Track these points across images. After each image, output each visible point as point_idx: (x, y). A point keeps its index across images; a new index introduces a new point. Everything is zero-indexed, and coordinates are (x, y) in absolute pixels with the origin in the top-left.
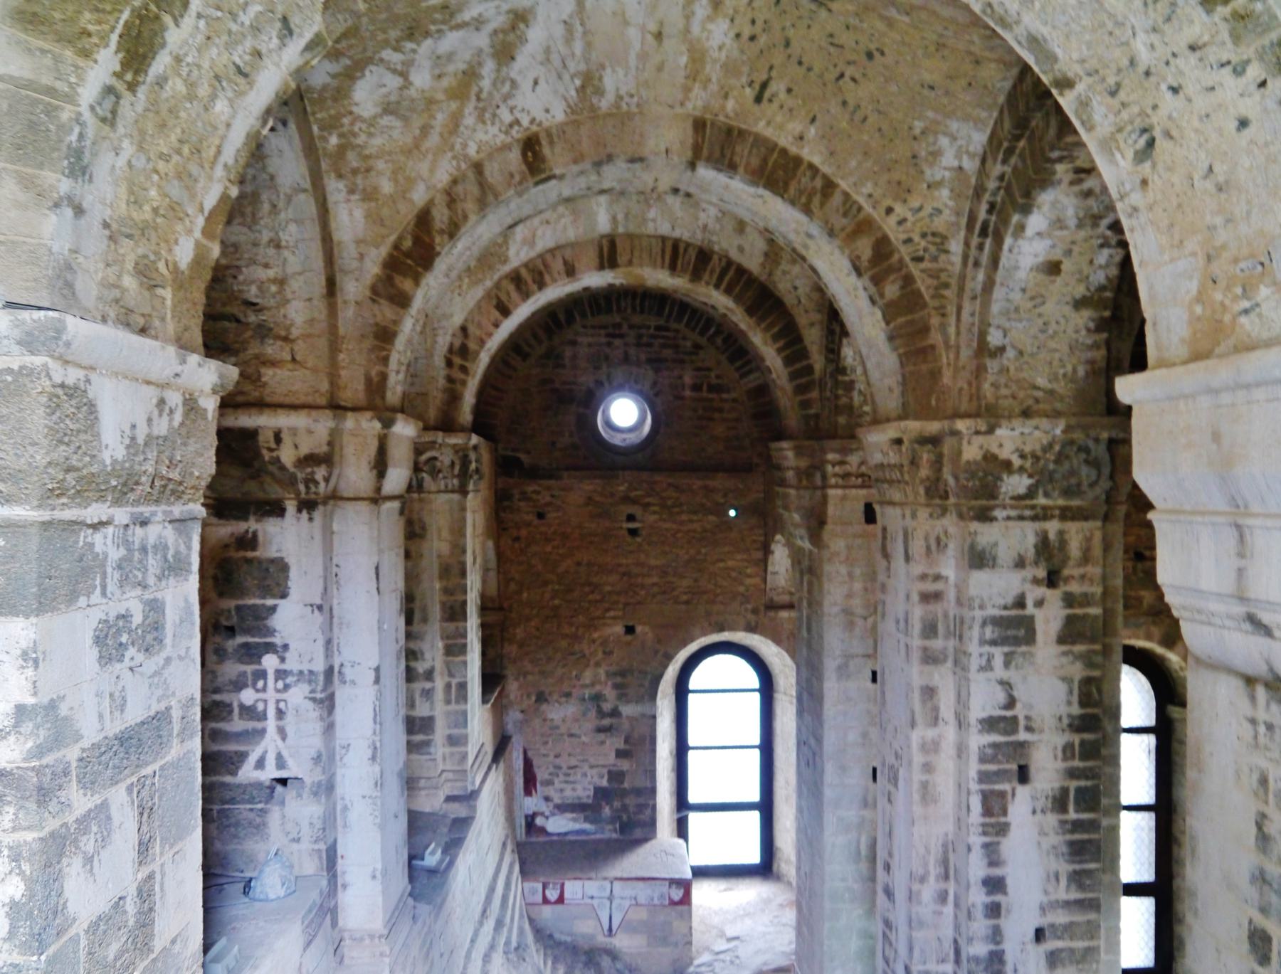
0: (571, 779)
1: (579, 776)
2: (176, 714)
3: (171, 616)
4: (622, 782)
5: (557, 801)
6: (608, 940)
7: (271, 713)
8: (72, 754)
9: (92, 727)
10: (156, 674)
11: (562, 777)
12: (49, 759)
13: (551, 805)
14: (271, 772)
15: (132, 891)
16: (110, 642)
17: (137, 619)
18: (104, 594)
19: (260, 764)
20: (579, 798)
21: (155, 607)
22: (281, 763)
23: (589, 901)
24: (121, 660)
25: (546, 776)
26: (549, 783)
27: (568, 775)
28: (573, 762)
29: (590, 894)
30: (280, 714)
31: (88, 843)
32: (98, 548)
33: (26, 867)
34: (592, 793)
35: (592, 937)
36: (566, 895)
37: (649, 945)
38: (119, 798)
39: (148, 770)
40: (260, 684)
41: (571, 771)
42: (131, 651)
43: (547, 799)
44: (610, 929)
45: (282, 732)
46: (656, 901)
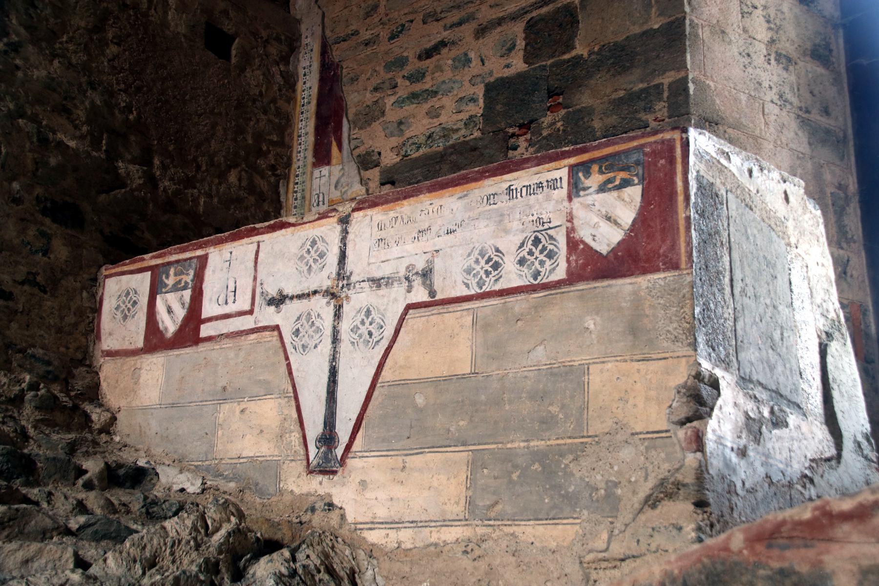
0: (427, 84)
1: (448, 74)
4: (570, 47)
5: (389, 159)
6: (318, 485)
11: (404, 88)
13: (374, 174)
20: (446, 132)
23: (267, 316)
25: (369, 98)
26: (371, 115)
27: (417, 77)
28: (437, 33)
29: (273, 292)
34: (477, 109)
35: (271, 468)
36: (209, 309)
37: (473, 510)
41: (429, 63)
43: (366, 162)
44: (328, 438)
46: (513, 276)
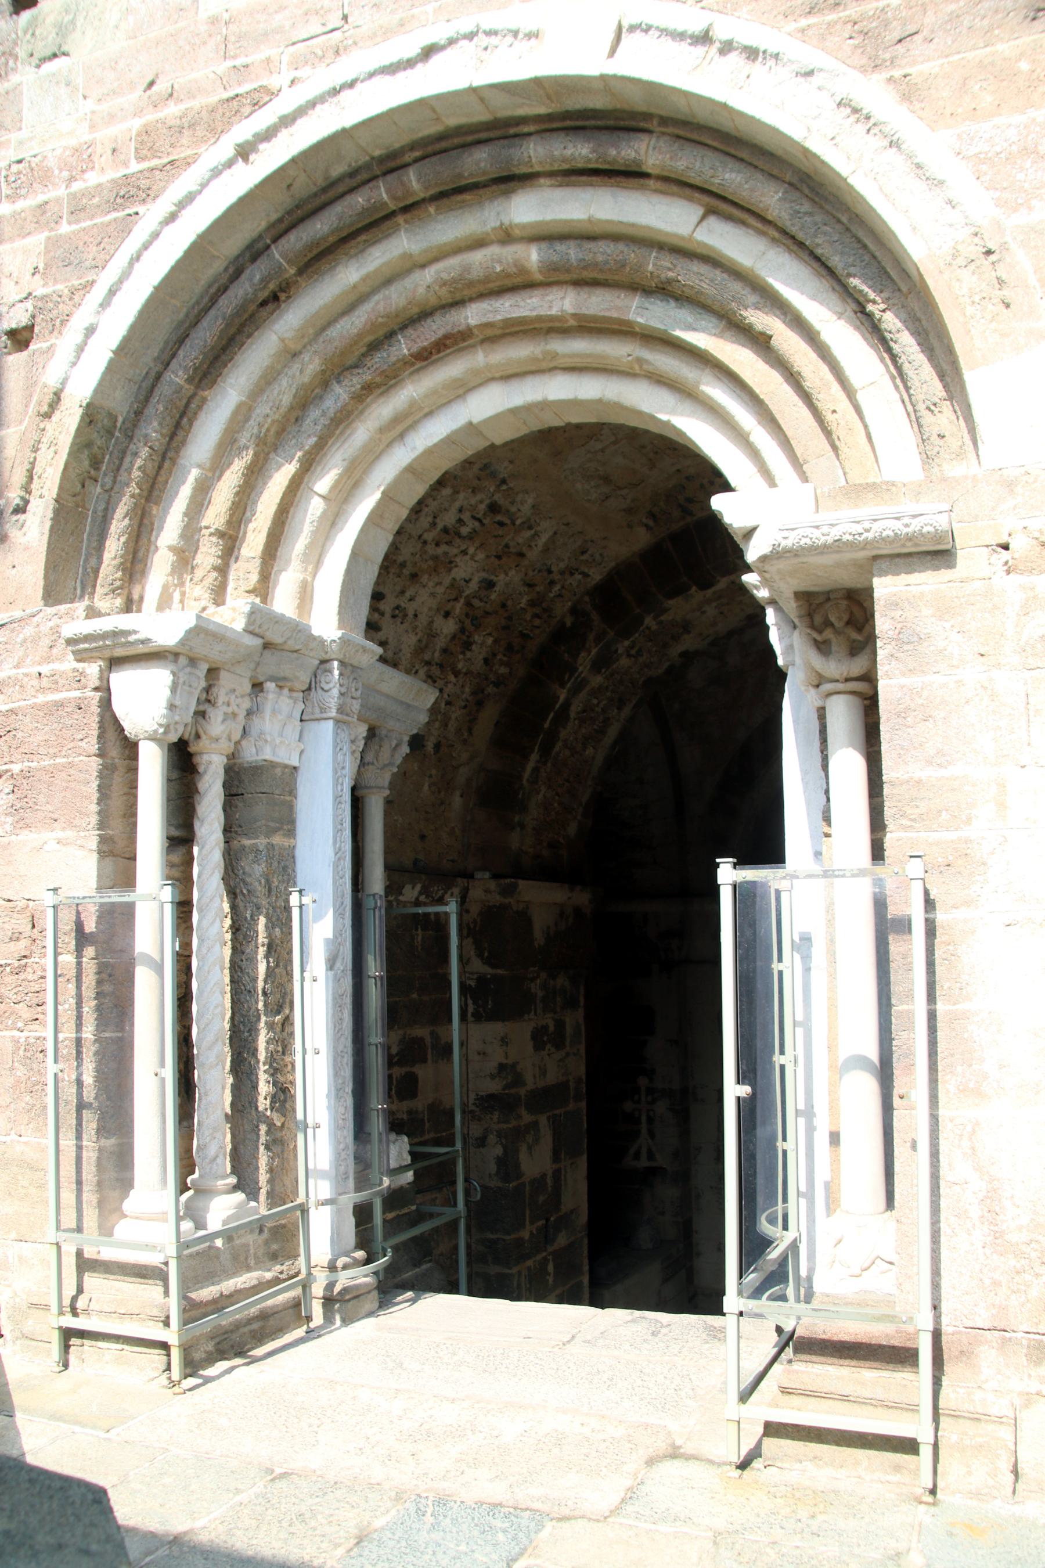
2: (572, 1085)
3: (569, 1030)
7: (644, 1119)
8: (522, 1092)
9: (531, 1081)
10: (560, 1060)
12: (513, 1091)
14: (644, 1163)
15: (550, 1173)
16: (539, 1038)
17: (552, 1028)
18: (536, 1014)
19: (637, 1156)
21: (560, 1024)
22: (651, 1156)
24: (544, 1050)
30: (650, 1120)
31: (530, 1139)
32: (533, 990)
33: (504, 1141)
38: (543, 1120)
39: (557, 1112)
40: (636, 1097)
42: (548, 1046)
45: (651, 1134)
